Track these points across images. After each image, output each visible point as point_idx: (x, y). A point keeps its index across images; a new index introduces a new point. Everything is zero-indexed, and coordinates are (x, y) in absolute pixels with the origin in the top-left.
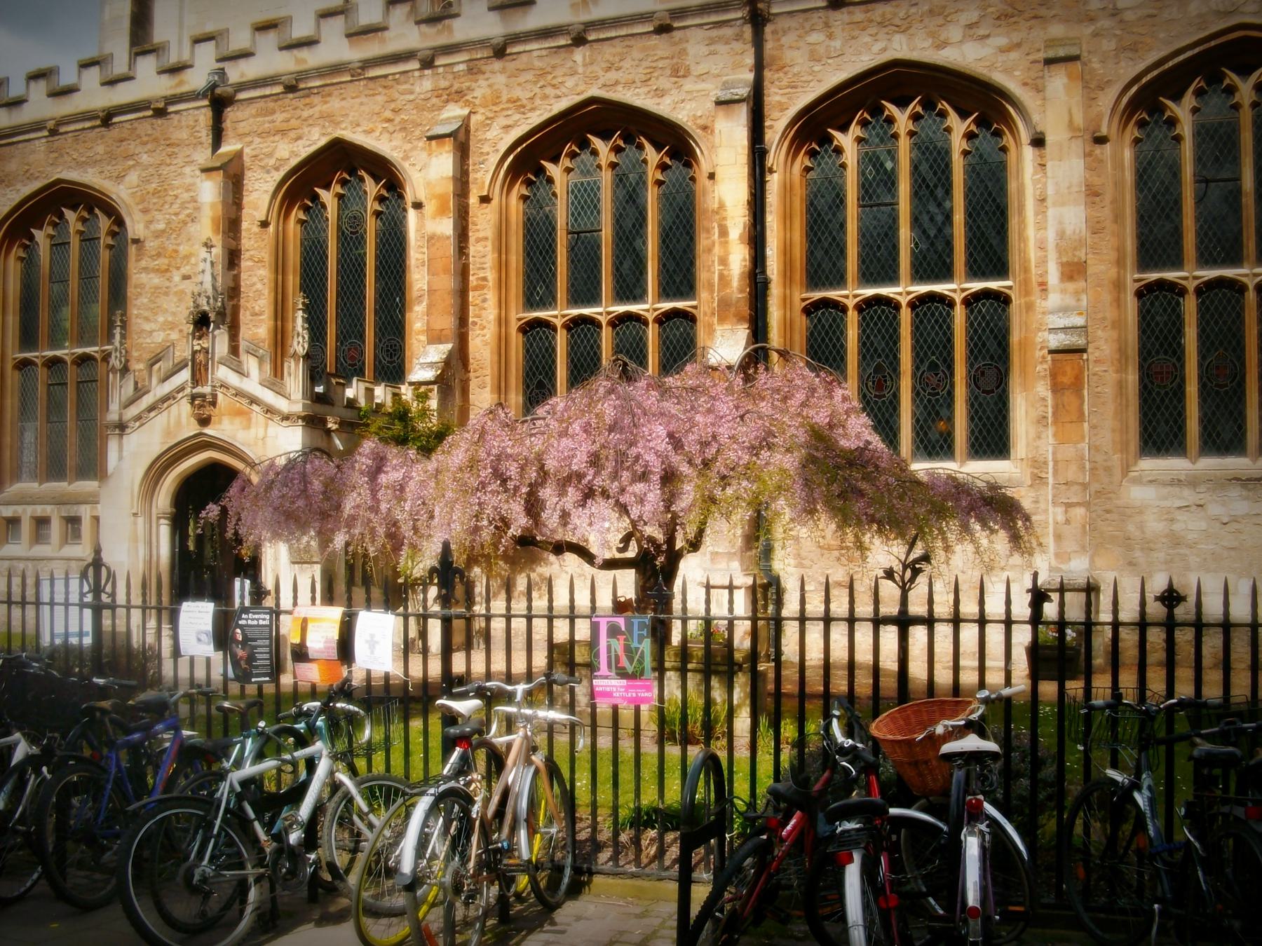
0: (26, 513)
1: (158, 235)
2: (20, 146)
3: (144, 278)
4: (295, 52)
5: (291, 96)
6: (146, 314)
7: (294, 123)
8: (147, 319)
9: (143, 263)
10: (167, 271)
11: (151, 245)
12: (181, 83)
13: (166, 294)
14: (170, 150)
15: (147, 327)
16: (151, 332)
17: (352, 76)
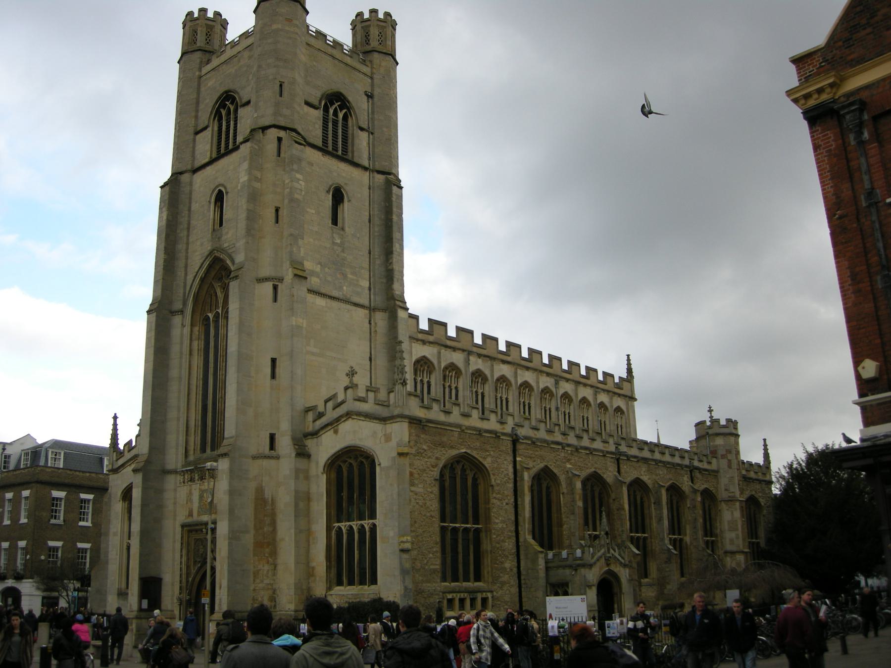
0: (457, 596)
1: (498, 485)
2: (449, 431)
3: (495, 501)
4: (534, 431)
5: (533, 445)
6: (496, 516)
7: (534, 456)
8: (496, 518)
9: (494, 495)
10: (501, 500)
11: (496, 488)
12: (504, 429)
13: (501, 509)
14: (500, 453)
15: (497, 521)
16: (497, 523)
17: (548, 444)
